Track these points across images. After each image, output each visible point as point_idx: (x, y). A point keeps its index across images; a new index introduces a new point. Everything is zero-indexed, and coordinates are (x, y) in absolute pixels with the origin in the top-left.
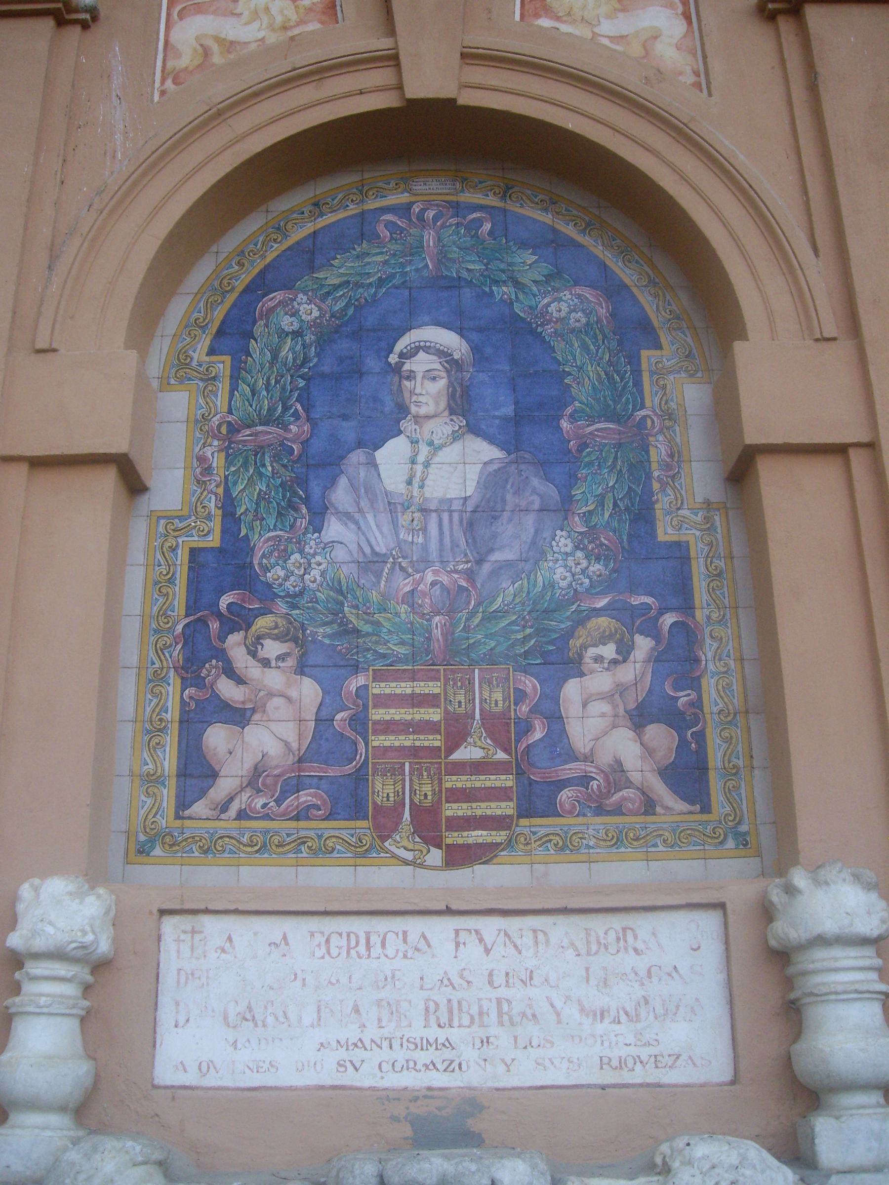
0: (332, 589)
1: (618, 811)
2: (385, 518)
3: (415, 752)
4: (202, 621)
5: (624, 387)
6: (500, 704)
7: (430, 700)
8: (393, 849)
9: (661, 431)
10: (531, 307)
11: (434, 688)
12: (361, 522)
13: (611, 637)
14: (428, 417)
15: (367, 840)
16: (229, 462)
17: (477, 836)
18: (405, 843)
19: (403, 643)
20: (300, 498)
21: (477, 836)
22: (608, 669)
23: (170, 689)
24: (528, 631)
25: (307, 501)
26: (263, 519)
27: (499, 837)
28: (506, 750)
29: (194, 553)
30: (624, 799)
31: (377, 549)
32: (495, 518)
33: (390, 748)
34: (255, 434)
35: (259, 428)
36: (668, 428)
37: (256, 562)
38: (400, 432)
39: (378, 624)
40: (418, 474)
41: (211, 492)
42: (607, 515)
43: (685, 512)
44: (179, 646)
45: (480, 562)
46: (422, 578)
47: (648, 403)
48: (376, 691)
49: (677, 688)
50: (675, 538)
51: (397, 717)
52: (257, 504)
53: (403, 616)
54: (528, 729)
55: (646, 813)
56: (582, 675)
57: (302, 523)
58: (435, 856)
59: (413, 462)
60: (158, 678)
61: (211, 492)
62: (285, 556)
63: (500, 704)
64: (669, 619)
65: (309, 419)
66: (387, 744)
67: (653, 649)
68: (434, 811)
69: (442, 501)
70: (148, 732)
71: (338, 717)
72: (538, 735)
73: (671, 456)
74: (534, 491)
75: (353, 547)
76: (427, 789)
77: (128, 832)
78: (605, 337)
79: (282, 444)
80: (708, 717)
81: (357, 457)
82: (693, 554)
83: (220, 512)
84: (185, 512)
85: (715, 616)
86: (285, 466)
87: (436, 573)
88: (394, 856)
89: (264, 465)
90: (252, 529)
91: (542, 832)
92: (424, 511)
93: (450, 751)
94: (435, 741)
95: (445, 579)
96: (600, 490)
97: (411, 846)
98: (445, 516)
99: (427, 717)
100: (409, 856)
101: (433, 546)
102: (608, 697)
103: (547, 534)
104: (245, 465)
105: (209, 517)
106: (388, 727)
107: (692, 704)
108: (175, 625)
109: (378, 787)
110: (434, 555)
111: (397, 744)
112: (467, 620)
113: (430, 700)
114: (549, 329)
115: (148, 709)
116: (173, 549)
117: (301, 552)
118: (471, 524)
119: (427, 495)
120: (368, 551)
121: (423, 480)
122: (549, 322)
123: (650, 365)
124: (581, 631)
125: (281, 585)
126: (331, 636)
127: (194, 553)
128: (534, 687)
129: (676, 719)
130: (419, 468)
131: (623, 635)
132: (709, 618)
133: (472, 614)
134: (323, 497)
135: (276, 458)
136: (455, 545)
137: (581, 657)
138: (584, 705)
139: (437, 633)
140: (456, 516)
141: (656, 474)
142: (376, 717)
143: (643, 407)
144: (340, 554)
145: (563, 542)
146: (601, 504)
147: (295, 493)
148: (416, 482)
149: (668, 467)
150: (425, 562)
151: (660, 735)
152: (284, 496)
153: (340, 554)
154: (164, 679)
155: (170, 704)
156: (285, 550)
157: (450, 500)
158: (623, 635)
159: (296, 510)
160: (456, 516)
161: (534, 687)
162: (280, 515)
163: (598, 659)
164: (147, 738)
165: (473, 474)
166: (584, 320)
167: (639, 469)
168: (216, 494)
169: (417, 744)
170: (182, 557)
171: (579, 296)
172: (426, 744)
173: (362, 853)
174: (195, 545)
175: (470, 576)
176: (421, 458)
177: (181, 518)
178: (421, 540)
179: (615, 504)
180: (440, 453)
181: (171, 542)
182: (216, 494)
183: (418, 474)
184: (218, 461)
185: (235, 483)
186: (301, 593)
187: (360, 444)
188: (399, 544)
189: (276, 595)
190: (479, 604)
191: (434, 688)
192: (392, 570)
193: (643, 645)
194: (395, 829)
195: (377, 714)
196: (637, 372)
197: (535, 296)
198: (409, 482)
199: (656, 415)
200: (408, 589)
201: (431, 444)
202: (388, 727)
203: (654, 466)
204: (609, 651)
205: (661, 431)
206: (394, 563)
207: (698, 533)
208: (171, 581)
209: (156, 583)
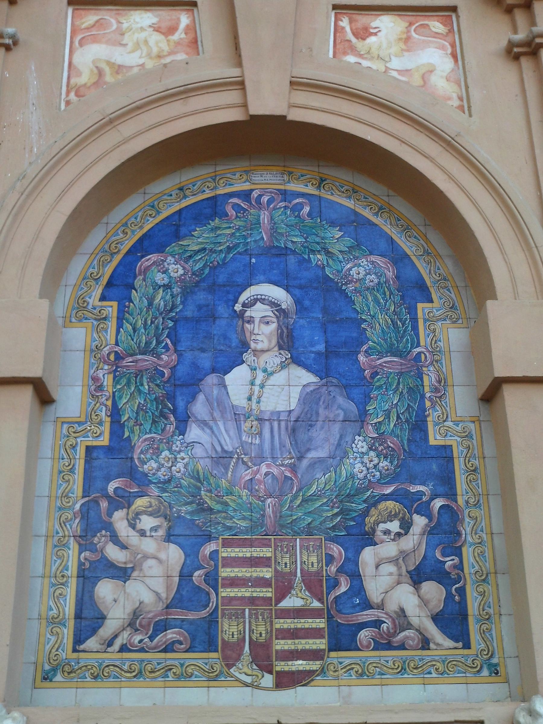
0: (192, 478)
1: (402, 647)
2: (231, 425)
3: (252, 601)
4: (96, 502)
5: (405, 331)
6: (315, 565)
7: (263, 562)
8: (237, 674)
9: (432, 363)
10: (338, 271)
11: (267, 552)
12: (215, 428)
13: (396, 516)
14: (263, 351)
15: (217, 667)
16: (116, 380)
17: (300, 665)
18: (246, 670)
19: (244, 518)
20: (169, 409)
21: (300, 665)
22: (393, 540)
23: (71, 552)
24: (336, 511)
25: (174, 412)
26: (141, 424)
27: (315, 665)
28: (320, 600)
29: (89, 449)
30: (407, 637)
31: (226, 448)
32: (311, 426)
33: (235, 598)
34: (136, 361)
35: (139, 357)
36: (437, 361)
37: (135, 457)
38: (243, 362)
39: (226, 504)
40: (256, 393)
41: (102, 404)
42: (392, 425)
43: (449, 423)
44: (77, 521)
45: (300, 458)
46: (258, 470)
47: (422, 343)
48: (225, 555)
49: (444, 555)
50: (442, 443)
51: (240, 575)
52: (137, 413)
53: (244, 498)
54: (336, 584)
55: (423, 648)
56: (375, 544)
57: (171, 428)
58: (268, 680)
59: (252, 384)
60: (61, 545)
61: (102, 404)
62: (157, 452)
63: (315, 565)
64: (438, 503)
65: (176, 351)
66: (232, 594)
67: (427, 525)
68: (267, 646)
69: (272, 413)
70: (54, 585)
71: (196, 574)
72: (343, 588)
73: (439, 382)
74: (339, 407)
75: (208, 446)
76: (262, 629)
77: (36, 663)
78: (391, 293)
79: (156, 369)
80: (467, 576)
81: (212, 379)
82: (455, 455)
83: (109, 419)
84: (83, 419)
85: (472, 501)
86: (157, 385)
87: (268, 466)
88: (238, 680)
89: (142, 385)
90: (133, 432)
91: (347, 662)
92: (260, 420)
93: (278, 601)
94: (268, 593)
95: (275, 471)
96: (387, 407)
97: (250, 672)
98: (276, 424)
99: (261, 575)
100: (248, 680)
101: (267, 446)
102: (394, 561)
103: (349, 439)
104: (128, 384)
105: (101, 423)
106: (233, 582)
107: (455, 567)
108: (74, 504)
109: (226, 626)
110: (267, 454)
111: (240, 595)
112: (291, 501)
113: (263, 562)
114: (351, 287)
115: (54, 569)
116: (73, 447)
117: (170, 449)
118: (294, 430)
119: (263, 409)
120: (219, 449)
121: (259, 398)
122: (351, 282)
123: (424, 314)
124: (373, 511)
125: (154, 474)
126: (192, 513)
127: (89, 449)
128: (340, 553)
130: (256, 389)
131: (404, 514)
132: (467, 502)
133: (295, 497)
134: (186, 408)
135: (151, 379)
136: (282, 445)
137: (374, 531)
138: (377, 567)
139: (269, 511)
140: (283, 424)
141: (428, 395)
142: (224, 575)
143: (418, 345)
144: (198, 451)
145: (361, 445)
146: (388, 416)
147: (166, 406)
148: (254, 398)
149: (437, 390)
150: (260, 458)
152: (157, 408)
153: (198, 451)
154: (66, 546)
155: (70, 564)
156: (158, 448)
157: (279, 413)
158: (404, 514)
159: (166, 418)
160: (283, 424)
161: (340, 553)
162: (154, 422)
163: (387, 532)
164: (52, 590)
165: (295, 393)
166: (376, 281)
168: (106, 406)
169: (255, 595)
170: (81, 452)
171: (373, 263)
172: (261, 595)
174: (89, 444)
175: (293, 468)
176: (258, 382)
177: (79, 423)
178: (257, 441)
179: (398, 417)
180: (272, 378)
181: (72, 441)
182: (106, 406)
183: (256, 393)
184: (108, 381)
185: (121, 398)
186: (169, 481)
187: (214, 370)
188: (242, 444)
189: (151, 482)
190: (300, 490)
191: (267, 552)
192: (237, 463)
193: (420, 522)
194: (238, 659)
195: (225, 572)
196: (414, 320)
197: (341, 262)
198: (250, 399)
199: (429, 351)
200: (248, 478)
201: (265, 371)
202: (233, 582)
203: (427, 389)
204: (394, 526)
205: (432, 363)
206: (238, 458)
207: (459, 439)
208: (72, 471)
209: (60, 472)
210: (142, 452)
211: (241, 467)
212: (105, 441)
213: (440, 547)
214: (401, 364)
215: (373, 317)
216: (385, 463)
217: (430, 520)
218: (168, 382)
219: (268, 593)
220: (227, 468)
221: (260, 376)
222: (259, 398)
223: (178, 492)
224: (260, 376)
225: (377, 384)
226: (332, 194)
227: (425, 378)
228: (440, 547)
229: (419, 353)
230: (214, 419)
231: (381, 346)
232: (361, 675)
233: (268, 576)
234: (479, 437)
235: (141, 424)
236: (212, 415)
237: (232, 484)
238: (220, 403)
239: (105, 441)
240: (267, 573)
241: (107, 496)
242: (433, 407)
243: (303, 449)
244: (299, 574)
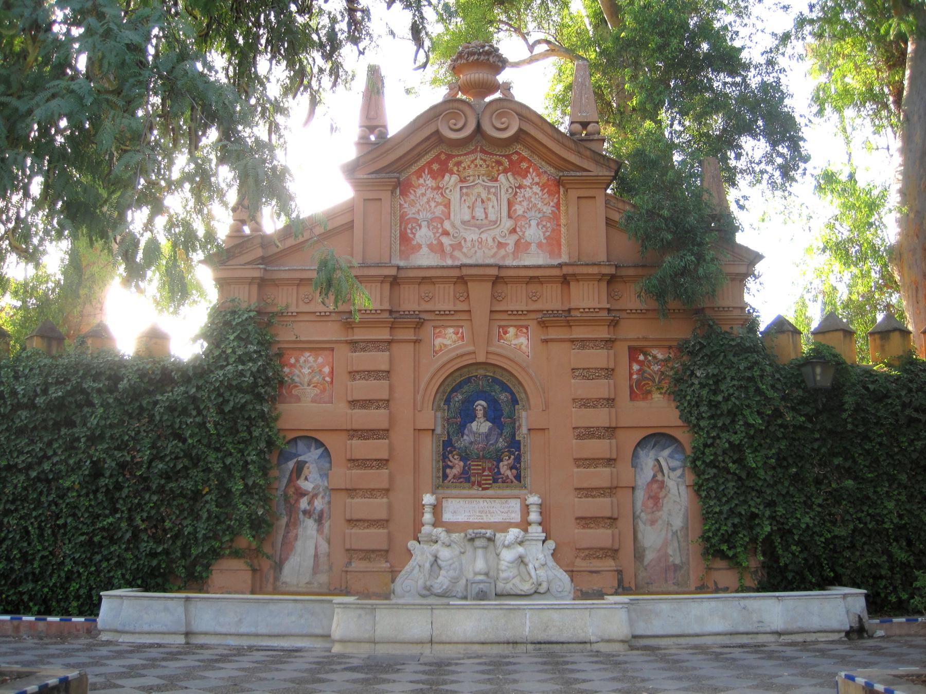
129: (517, 469)
151: (514, 471)
167: (514, 428)
173: (470, 488)
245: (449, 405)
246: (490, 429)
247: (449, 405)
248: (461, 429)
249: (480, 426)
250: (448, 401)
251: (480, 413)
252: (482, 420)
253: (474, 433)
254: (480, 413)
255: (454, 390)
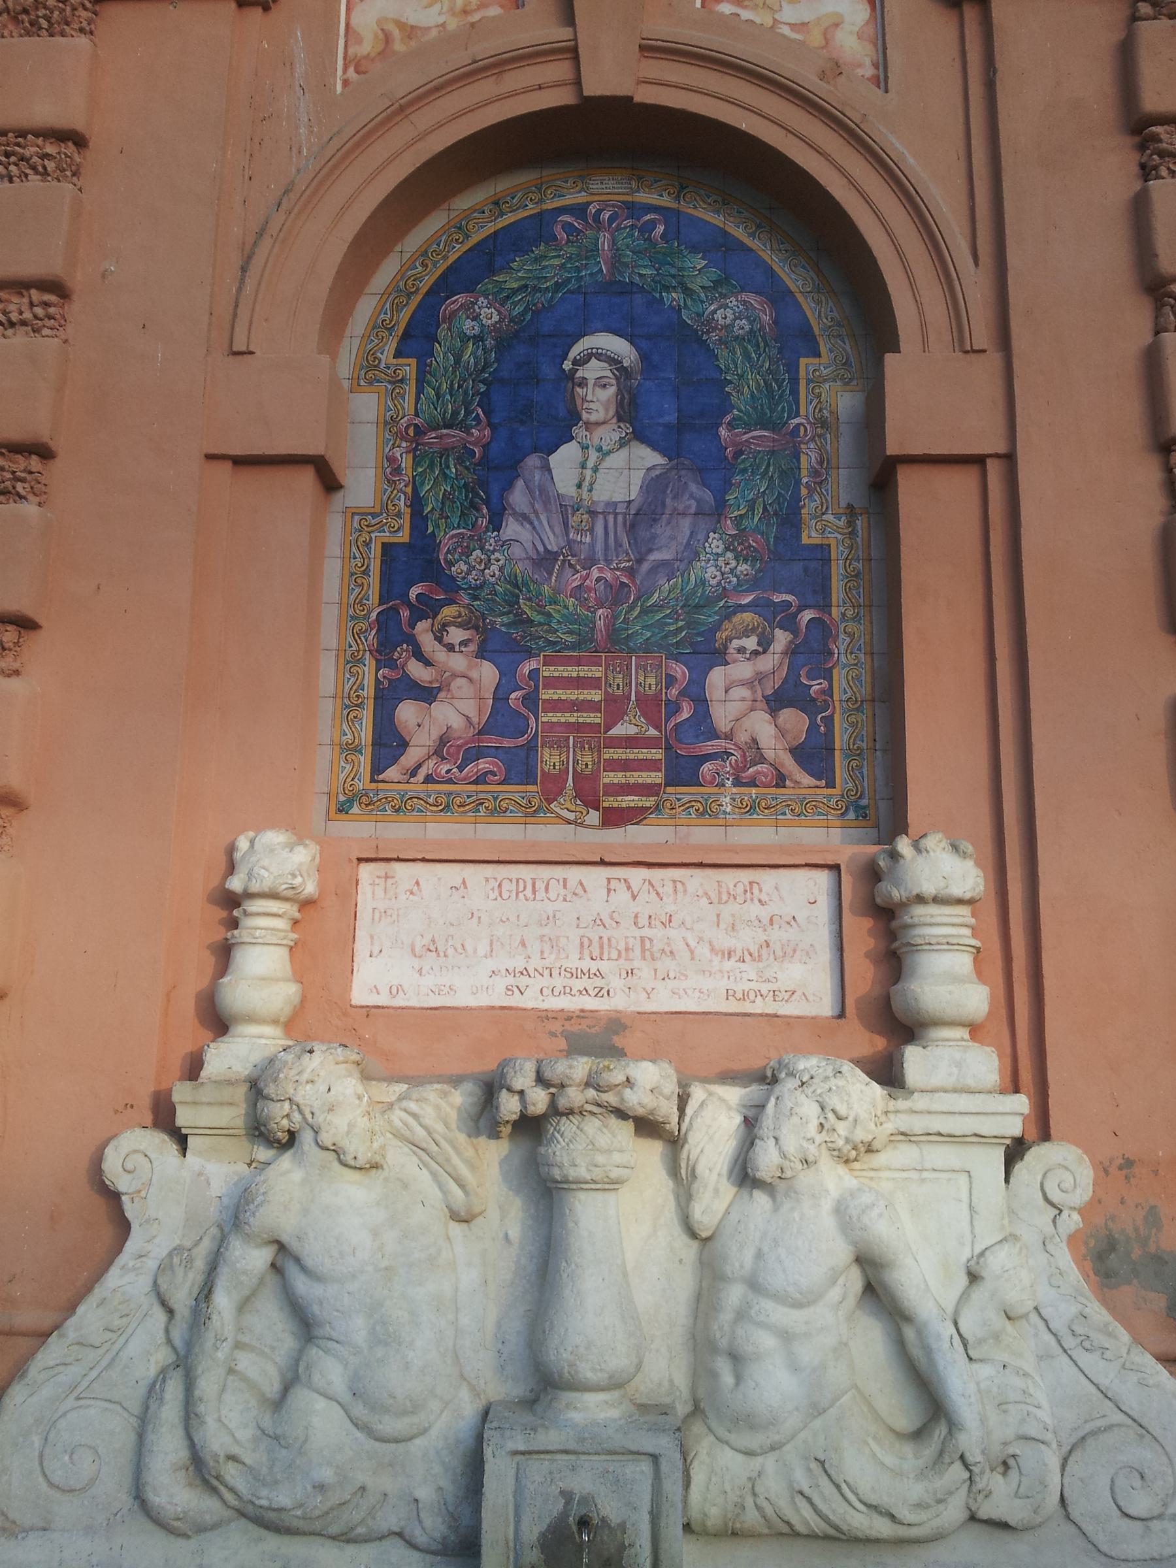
0: (509, 583)
1: (753, 783)
2: (557, 519)
3: (577, 727)
4: (395, 609)
7: (594, 683)
8: (558, 810)
9: (812, 439)
10: (698, 315)
11: (597, 672)
12: (536, 523)
13: (753, 630)
14: (598, 424)
16: (416, 463)
18: (568, 805)
19: (570, 632)
20: (482, 499)
23: (366, 669)
24: (681, 624)
27: (649, 802)
28: (657, 728)
29: (385, 546)
30: (759, 773)
31: (549, 548)
32: (655, 520)
33: (559, 724)
35: (444, 431)
36: (820, 436)
37: (441, 557)
39: (549, 615)
40: (588, 478)
41: (401, 491)
42: (756, 519)
44: (374, 632)
45: (640, 561)
46: (588, 575)
47: (803, 411)
48: (546, 674)
49: (810, 678)
52: (443, 503)
53: (571, 609)
54: (678, 710)
55: (777, 786)
58: (594, 817)
60: (356, 660)
61: (401, 491)
64: (807, 616)
65: (489, 424)
66: (554, 720)
67: (791, 642)
68: (595, 777)
69: (608, 504)
71: (513, 696)
72: (685, 715)
73: (821, 463)
74: (692, 496)
75: (528, 545)
76: (588, 759)
78: (766, 345)
79: (465, 447)
80: (837, 704)
81: (533, 461)
83: (409, 510)
86: (467, 468)
87: (600, 570)
88: (559, 816)
89: (448, 467)
91: (686, 798)
92: (592, 513)
93: (608, 728)
94: (596, 718)
95: (608, 576)
98: (611, 518)
100: (571, 816)
101: (599, 546)
102: (748, 684)
103: (701, 537)
104: (431, 466)
105: (399, 515)
106: (555, 706)
107: (823, 692)
108: (369, 613)
109: (546, 757)
110: (600, 555)
111: (563, 720)
112: (627, 613)
113: (594, 683)
114: (714, 337)
115: (347, 688)
116: (367, 544)
117: (482, 549)
118: (633, 526)
120: (541, 549)
122: (716, 328)
123: (807, 373)
124: (726, 624)
125: (464, 578)
127: (385, 546)
130: (588, 473)
131: (764, 629)
132: (843, 615)
133: (631, 608)
135: (460, 461)
136: (618, 545)
137: (726, 648)
139: (600, 624)
140: (620, 518)
141: (805, 480)
142: (545, 697)
144: (516, 551)
145: (715, 544)
146: (752, 508)
148: (586, 484)
151: (792, 718)
152: (467, 496)
153: (516, 551)
154: (361, 661)
155: (366, 682)
157: (615, 504)
158: (764, 629)
159: (478, 510)
160: (620, 518)
161: (684, 673)
162: (463, 514)
163: (741, 650)
165: (637, 478)
166: (747, 328)
168: (405, 493)
169: (581, 720)
170: (376, 551)
171: (744, 303)
172: (588, 720)
173: (531, 813)
175: (631, 572)
176: (590, 464)
178: (588, 540)
179: (765, 509)
181: (365, 536)
182: (405, 493)
184: (406, 462)
185: (423, 483)
186: (481, 587)
187: (535, 450)
188: (570, 543)
190: (637, 599)
191: (597, 672)
192: (562, 566)
193: (782, 638)
194: (560, 793)
195: (546, 694)
196: (795, 381)
197: (702, 302)
198: (579, 486)
199: (809, 423)
201: (600, 449)
202: (555, 706)
203: (804, 472)
204: (751, 643)
205: (812, 439)
207: (839, 536)
208: (366, 572)
209: (352, 575)
210: (448, 552)
211: (568, 571)
212: (404, 537)
213: (806, 669)
214: (774, 440)
215: (741, 377)
216: (745, 566)
217: (796, 637)
218: (478, 464)
219: (596, 718)
220: (550, 574)
221: (593, 456)
222: (591, 484)
223: (492, 600)
224: (593, 456)
225: (742, 466)
226: (695, 208)
227: (803, 458)
228: (806, 669)
229: (799, 425)
230: (536, 513)
231: (749, 416)
232: (702, 814)
233: (597, 698)
234: (866, 535)
235: (448, 517)
236: (533, 506)
237: (557, 591)
238: (543, 490)
239: (404, 537)
240: (596, 696)
241: (409, 605)
242: (810, 495)
243: (643, 550)
244: (633, 698)
245: (424, 357)
246: (655, 486)
247: (424, 357)
248: (487, 486)
249: (597, 467)
250: (418, 337)
251: (598, 400)
252: (609, 435)
253: (565, 510)
254: (598, 400)
255: (445, 286)
